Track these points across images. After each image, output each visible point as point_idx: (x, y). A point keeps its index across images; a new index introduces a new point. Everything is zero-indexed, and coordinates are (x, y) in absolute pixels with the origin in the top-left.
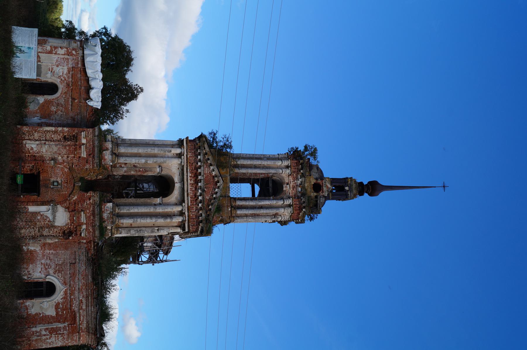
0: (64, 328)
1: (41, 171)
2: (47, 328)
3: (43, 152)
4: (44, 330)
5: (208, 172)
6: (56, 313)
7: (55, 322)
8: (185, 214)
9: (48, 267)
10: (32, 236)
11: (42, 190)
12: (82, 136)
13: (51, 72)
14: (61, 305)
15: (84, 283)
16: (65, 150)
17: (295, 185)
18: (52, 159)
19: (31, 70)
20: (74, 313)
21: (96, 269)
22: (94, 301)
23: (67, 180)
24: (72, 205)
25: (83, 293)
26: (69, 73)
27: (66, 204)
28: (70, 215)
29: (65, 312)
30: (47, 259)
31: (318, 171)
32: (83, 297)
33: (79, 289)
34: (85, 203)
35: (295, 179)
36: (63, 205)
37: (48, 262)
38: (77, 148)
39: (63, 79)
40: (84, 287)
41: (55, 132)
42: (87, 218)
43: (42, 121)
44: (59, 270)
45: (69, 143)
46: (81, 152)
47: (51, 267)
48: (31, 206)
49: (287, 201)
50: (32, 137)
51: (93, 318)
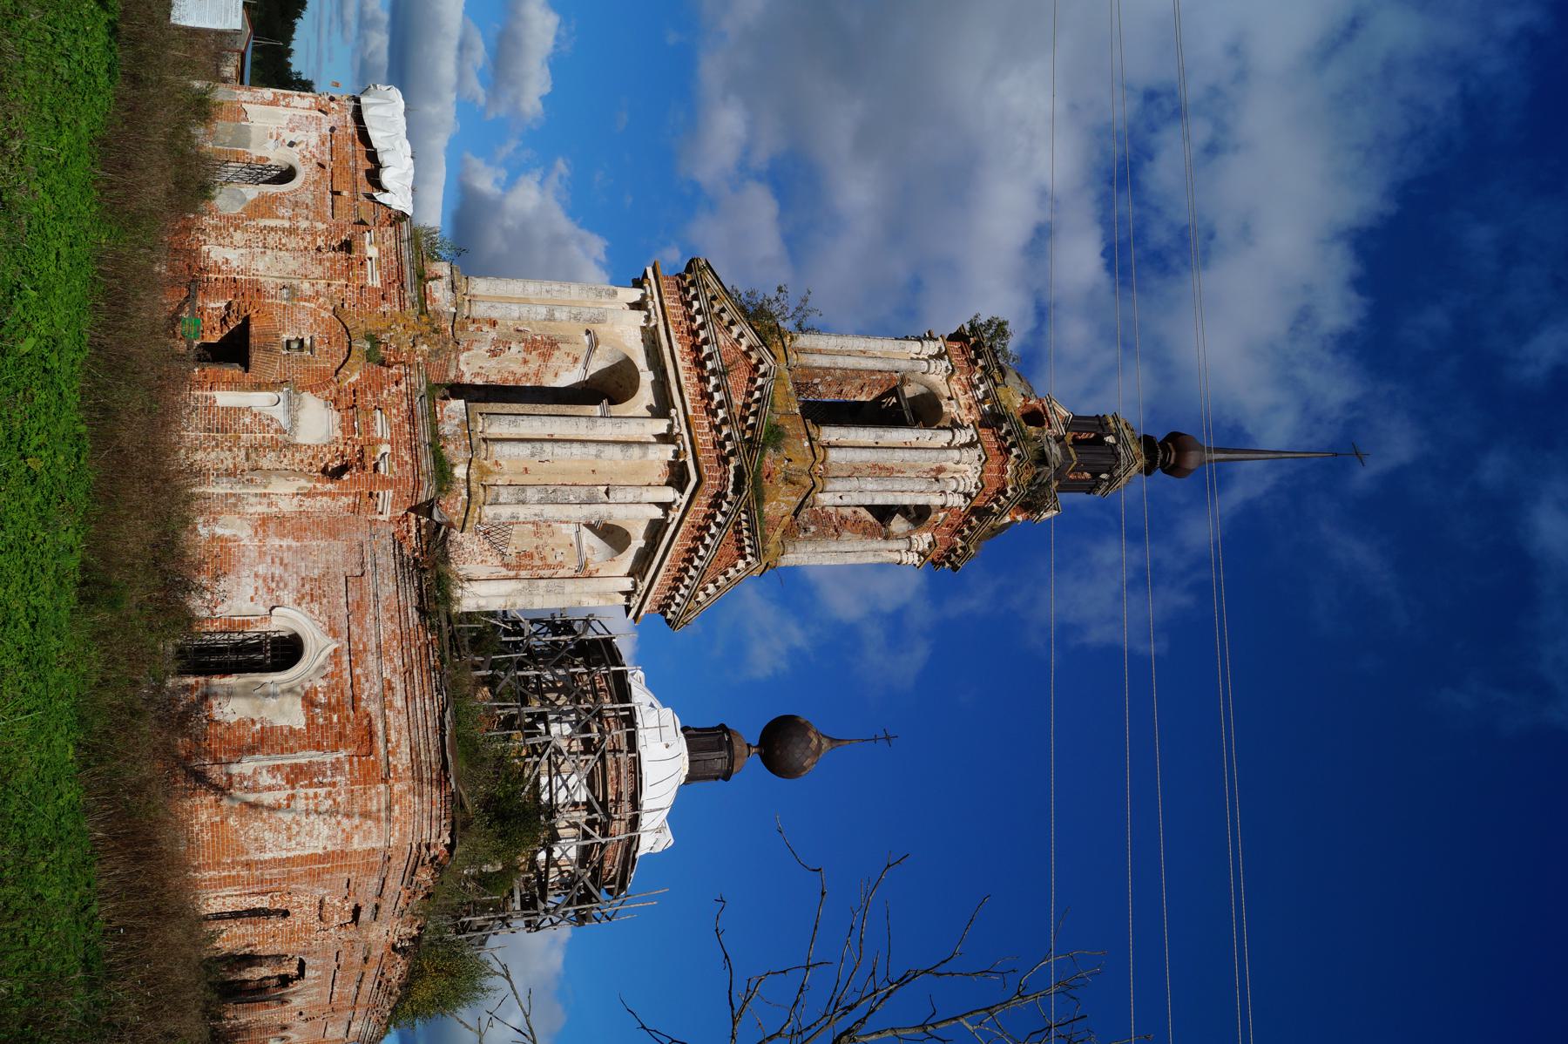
0: (336, 767)
2: (278, 766)
3: (257, 270)
4: (268, 771)
5: (728, 344)
6: (307, 719)
7: (303, 748)
9: (277, 586)
10: (226, 470)
11: (256, 356)
12: (368, 240)
14: (321, 696)
15: (393, 631)
20: (365, 722)
22: (430, 679)
23: (329, 338)
24: (346, 395)
25: (391, 660)
26: (323, 144)
27: (327, 392)
28: (343, 416)
29: (335, 718)
30: (273, 562)
32: (394, 671)
33: (379, 646)
37: (278, 571)
39: (308, 155)
40: (395, 643)
44: (312, 595)
46: (366, 275)
47: (286, 585)
48: (223, 390)
51: (430, 731)
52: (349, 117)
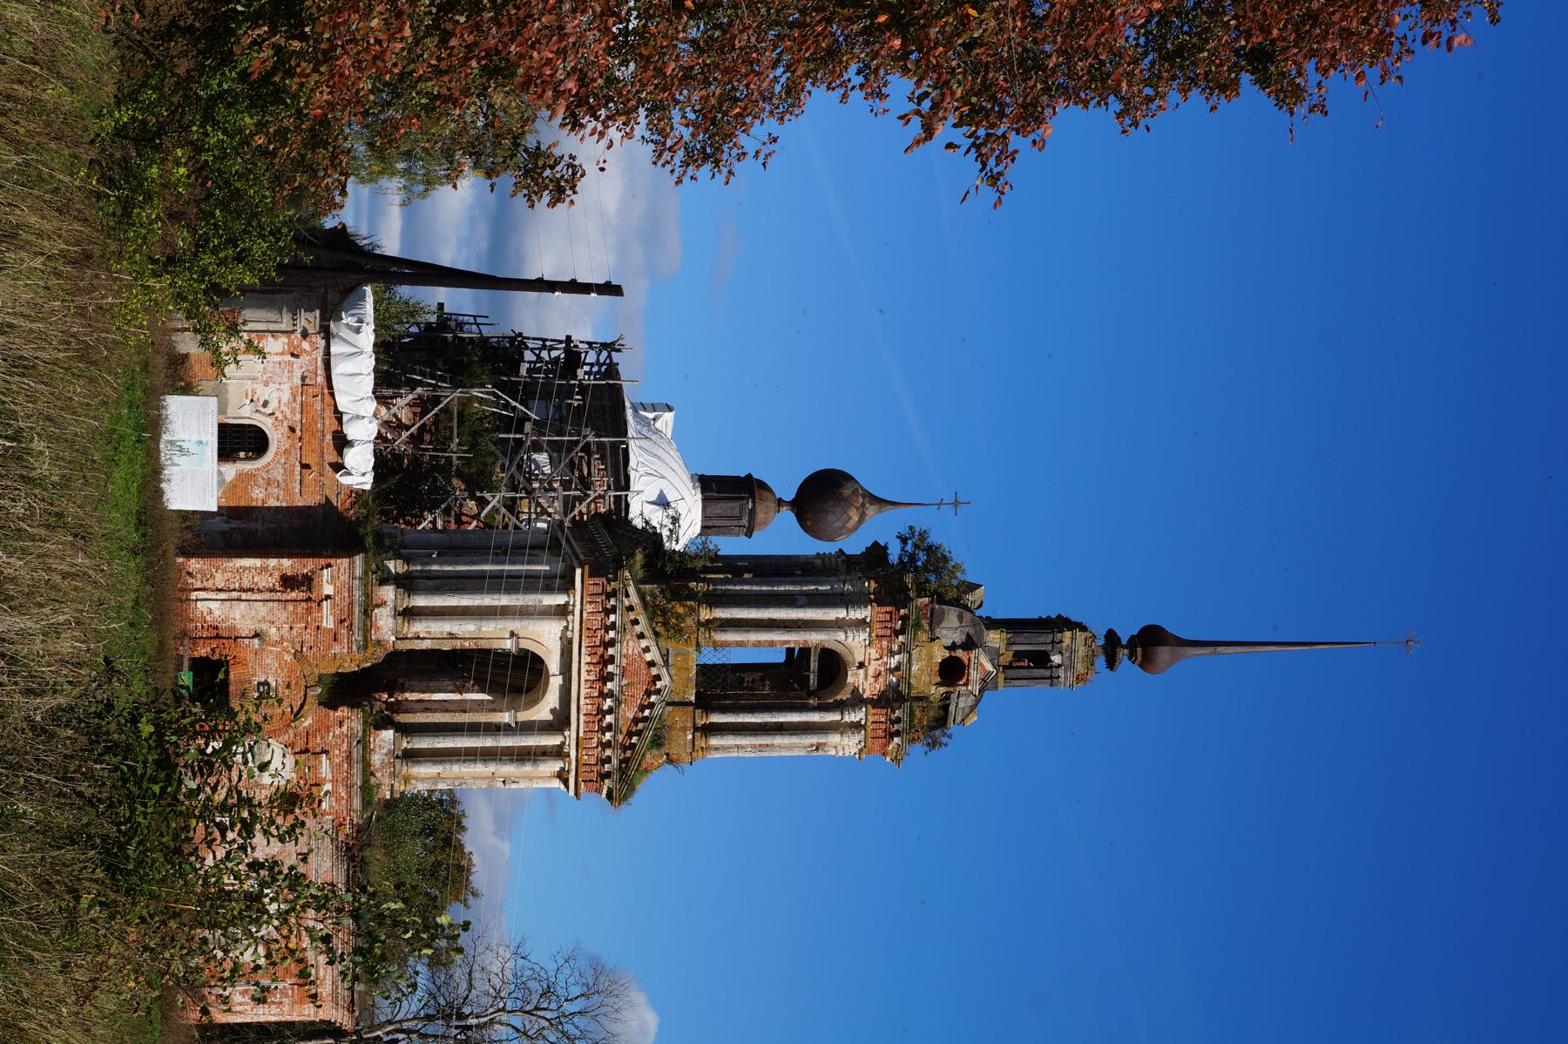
1: (232, 662)
5: (636, 652)
8: (569, 756)
12: (325, 578)
13: (252, 401)
16: (285, 614)
17: (882, 669)
18: (257, 635)
19: (204, 492)
21: (354, 872)
26: (295, 400)
27: (287, 737)
31: (961, 622)
34: (331, 734)
35: (885, 652)
36: (281, 739)
38: (311, 607)
39: (281, 418)
41: (263, 569)
42: (335, 768)
43: (232, 525)
45: (293, 595)
46: (322, 617)
49: (853, 714)
50: (211, 582)
52: (320, 359)
